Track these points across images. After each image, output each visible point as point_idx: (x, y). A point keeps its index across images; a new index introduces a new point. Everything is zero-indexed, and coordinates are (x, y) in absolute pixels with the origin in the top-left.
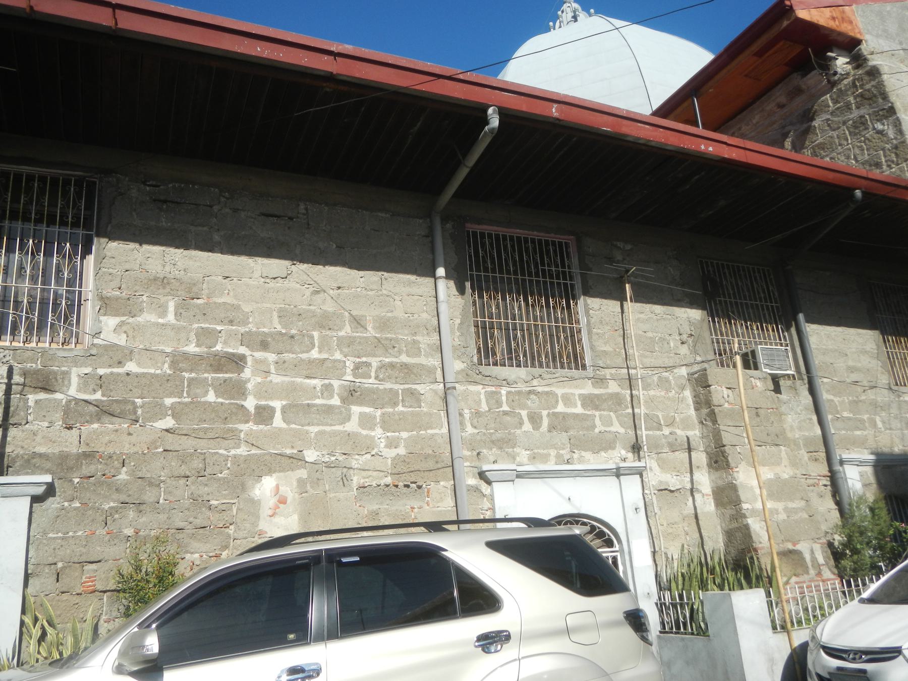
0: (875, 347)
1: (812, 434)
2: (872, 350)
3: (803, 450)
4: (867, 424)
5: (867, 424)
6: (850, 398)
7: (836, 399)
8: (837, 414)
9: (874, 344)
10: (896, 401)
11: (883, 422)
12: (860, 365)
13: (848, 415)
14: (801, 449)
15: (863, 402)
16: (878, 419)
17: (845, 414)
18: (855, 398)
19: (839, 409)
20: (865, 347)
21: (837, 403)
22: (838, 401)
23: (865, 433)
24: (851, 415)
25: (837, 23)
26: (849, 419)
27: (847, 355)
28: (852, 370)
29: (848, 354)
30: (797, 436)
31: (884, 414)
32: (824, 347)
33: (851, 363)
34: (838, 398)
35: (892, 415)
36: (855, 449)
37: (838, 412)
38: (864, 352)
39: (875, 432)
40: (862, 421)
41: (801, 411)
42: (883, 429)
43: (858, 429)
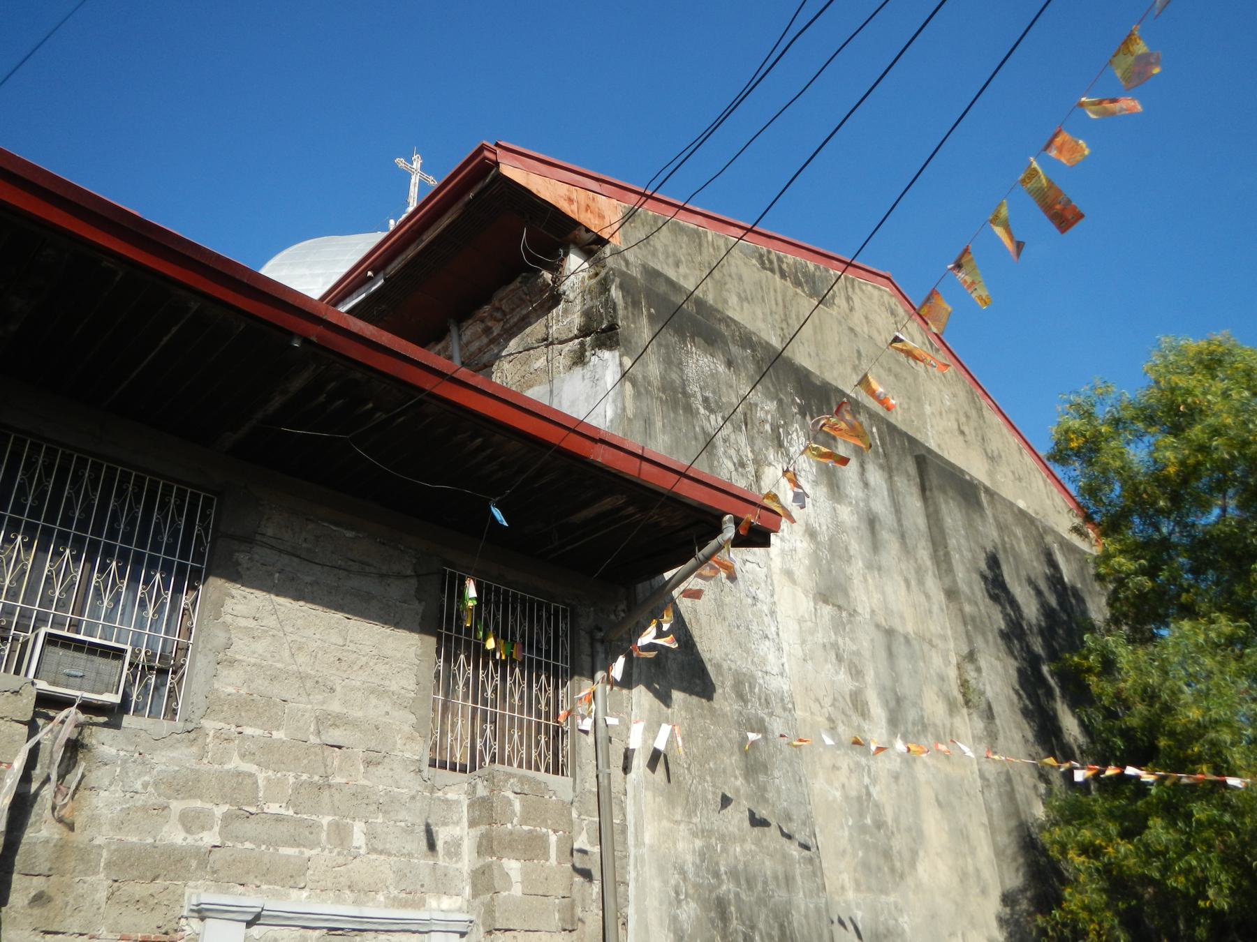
0: (413, 687)
1: (150, 840)
2: (403, 692)
3: (102, 876)
4: (324, 836)
5: (324, 836)
6: (304, 777)
7: (261, 777)
8: (250, 804)
9: (413, 680)
10: (425, 797)
11: (371, 835)
12: (360, 714)
13: (283, 811)
14: (95, 873)
15: (339, 788)
16: (358, 828)
17: (273, 808)
18: (316, 778)
19: (261, 794)
20: (387, 683)
21: (261, 783)
22: (268, 780)
23: (308, 853)
24: (291, 812)
25: (574, 207)
26: (279, 819)
27: (332, 690)
28: (338, 721)
29: (338, 689)
30: (99, 840)
31: (380, 820)
32: (279, 665)
33: (335, 707)
34: (270, 773)
35: (403, 824)
36: (264, 887)
37: (255, 801)
38: (380, 692)
39: (339, 854)
40: (312, 827)
41: (145, 786)
42: (362, 851)
43: (295, 842)
